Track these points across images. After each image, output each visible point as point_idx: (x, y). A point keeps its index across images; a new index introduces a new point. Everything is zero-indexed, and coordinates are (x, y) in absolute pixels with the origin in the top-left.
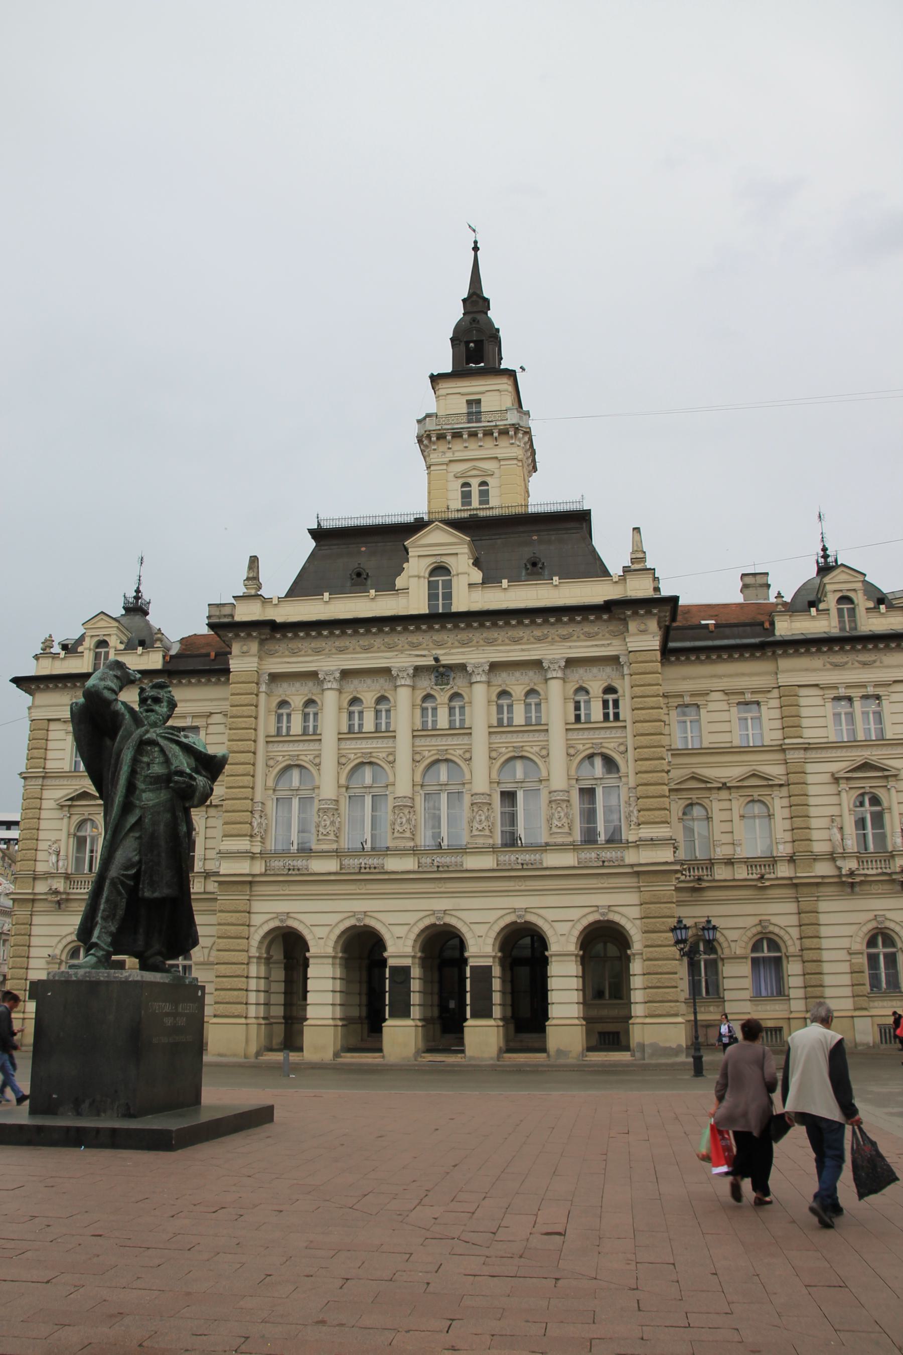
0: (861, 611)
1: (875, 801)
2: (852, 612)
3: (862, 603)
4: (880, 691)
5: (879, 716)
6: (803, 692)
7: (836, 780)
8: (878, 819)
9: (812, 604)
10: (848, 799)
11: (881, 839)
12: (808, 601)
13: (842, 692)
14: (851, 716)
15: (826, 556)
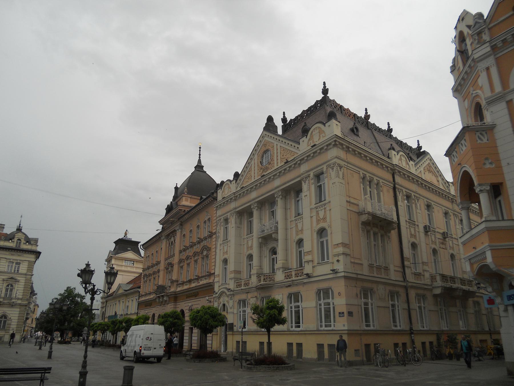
0: (22, 243)
1: (12, 286)
2: (20, 243)
3: (23, 241)
4: (21, 262)
5: (19, 267)
6: (2, 259)
7: (4, 280)
8: (11, 290)
9: (11, 239)
10: (5, 285)
11: (11, 295)
12: (10, 237)
13: (11, 260)
14: (12, 266)
15: (20, 226)
